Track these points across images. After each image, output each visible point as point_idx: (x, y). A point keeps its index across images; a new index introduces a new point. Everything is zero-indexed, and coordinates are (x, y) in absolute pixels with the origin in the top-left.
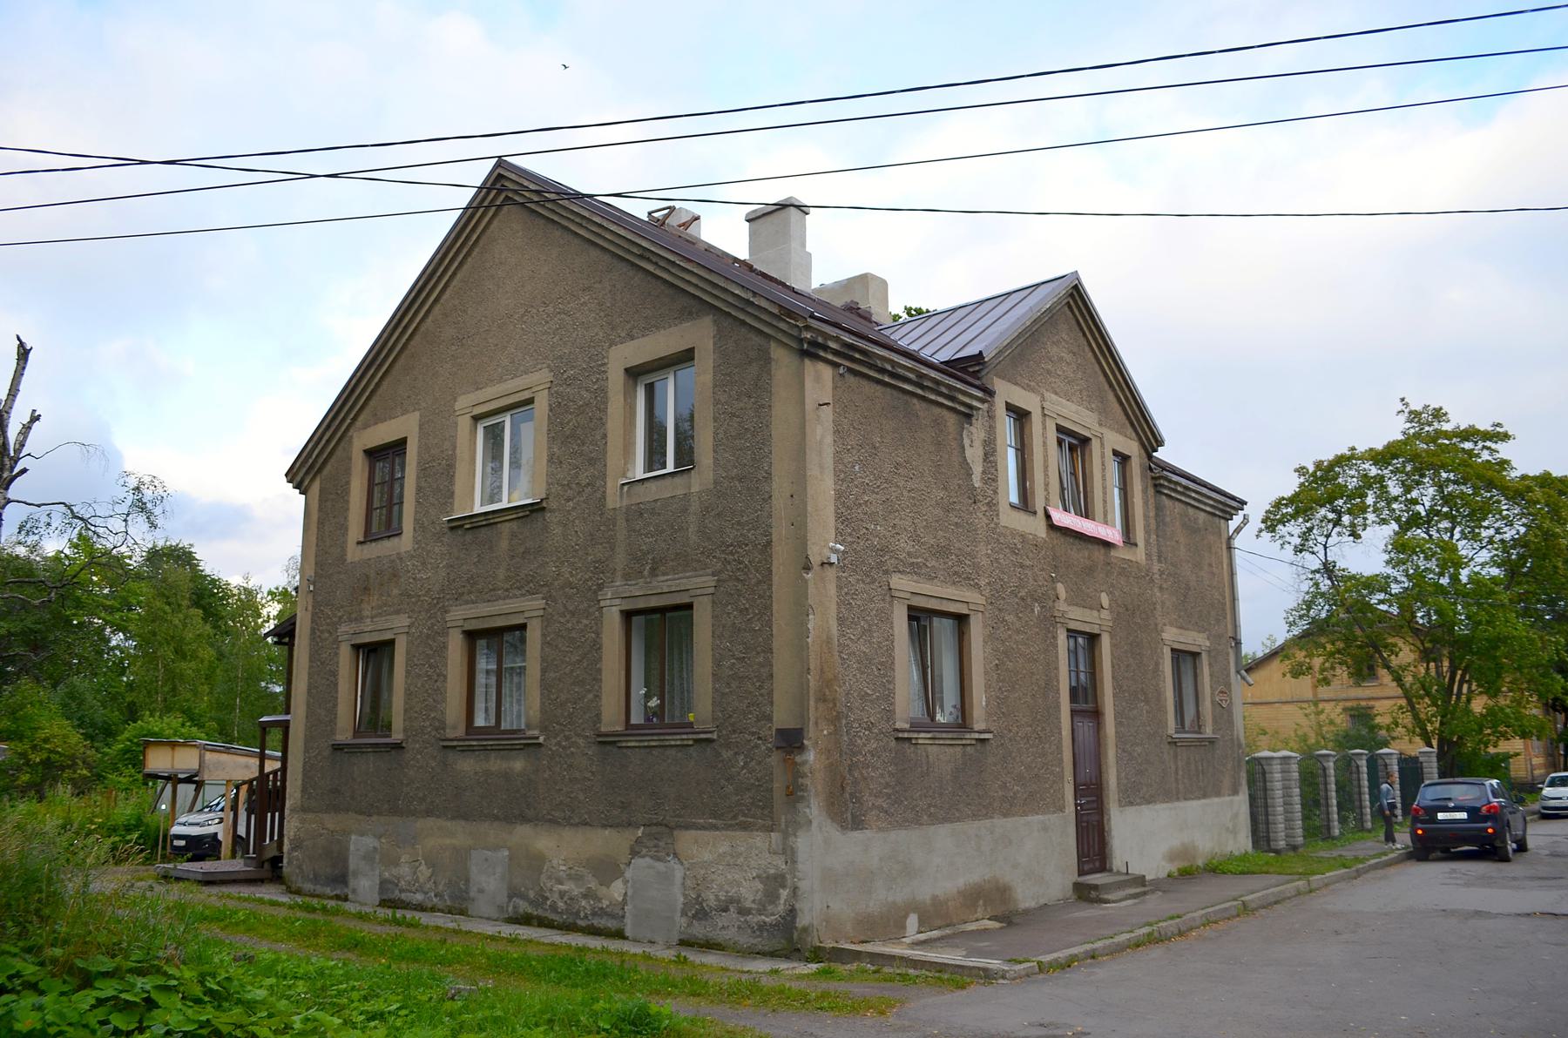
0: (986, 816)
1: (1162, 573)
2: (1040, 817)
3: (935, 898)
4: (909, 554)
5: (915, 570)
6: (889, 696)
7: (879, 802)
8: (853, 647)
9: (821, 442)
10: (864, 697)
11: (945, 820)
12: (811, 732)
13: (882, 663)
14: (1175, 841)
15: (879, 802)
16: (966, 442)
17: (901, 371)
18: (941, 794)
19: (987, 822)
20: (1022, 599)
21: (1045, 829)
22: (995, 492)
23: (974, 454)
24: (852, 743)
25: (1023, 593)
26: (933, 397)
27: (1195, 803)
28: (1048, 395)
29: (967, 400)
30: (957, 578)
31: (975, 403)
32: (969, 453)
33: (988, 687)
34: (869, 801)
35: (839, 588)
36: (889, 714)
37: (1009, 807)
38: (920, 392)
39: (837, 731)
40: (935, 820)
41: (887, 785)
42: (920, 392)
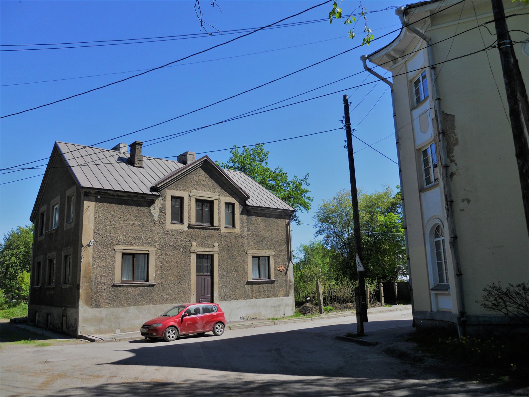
0: (154, 304)
1: (248, 235)
5: (125, 243)
7: (107, 301)
8: (98, 264)
9: (89, 215)
10: (101, 276)
11: (134, 305)
12: (81, 285)
15: (107, 301)
19: (154, 306)
20: (175, 247)
22: (164, 220)
25: (175, 246)
28: (192, 191)
30: (144, 244)
32: (152, 211)
34: (101, 300)
35: (94, 250)
36: (112, 280)
40: (129, 305)
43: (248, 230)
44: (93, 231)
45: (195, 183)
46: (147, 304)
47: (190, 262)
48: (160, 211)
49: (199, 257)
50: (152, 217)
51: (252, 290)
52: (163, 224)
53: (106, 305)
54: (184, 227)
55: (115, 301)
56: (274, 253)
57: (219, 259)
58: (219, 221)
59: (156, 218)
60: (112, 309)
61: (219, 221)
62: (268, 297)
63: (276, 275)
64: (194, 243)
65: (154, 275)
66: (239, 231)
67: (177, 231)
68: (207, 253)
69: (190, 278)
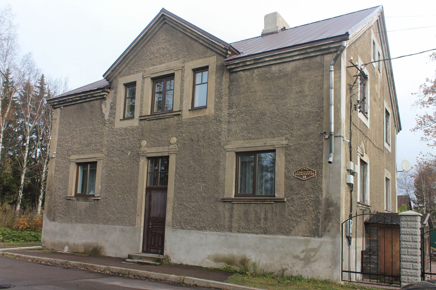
0: (96, 223)
1: (230, 115)
2: (122, 227)
3: (74, 244)
4: (77, 149)
5: (78, 153)
6: (66, 188)
7: (61, 215)
10: (59, 189)
11: (80, 222)
13: (65, 180)
14: (225, 252)
15: (61, 215)
16: (103, 106)
17: (74, 99)
18: (80, 215)
19: (97, 225)
20: (122, 151)
21: (123, 231)
22: (114, 118)
23: (106, 110)
24: (55, 200)
25: (123, 149)
26: (88, 100)
27: (249, 236)
29: (99, 94)
31: (101, 94)
32: (104, 111)
33: (102, 183)
34: (57, 214)
35: (56, 163)
36: (66, 193)
37: (107, 221)
38: (84, 101)
39: (51, 197)
40: (77, 222)
41: (63, 211)
42: (84, 101)
43: (230, 107)
44: (57, 143)
45: (152, 56)
46: (91, 223)
47: (139, 169)
48: (111, 108)
49: (154, 160)
50: (103, 115)
51: (231, 216)
52: (112, 123)
53: (60, 219)
54: (135, 123)
55: (66, 216)
56: (285, 142)
57: (177, 162)
58: (181, 102)
59: (106, 118)
60: (63, 224)
61: (181, 102)
62: (265, 232)
63: (289, 188)
64: (144, 143)
65: (100, 188)
66: (213, 111)
67: (126, 129)
68: (160, 155)
69: (136, 193)
